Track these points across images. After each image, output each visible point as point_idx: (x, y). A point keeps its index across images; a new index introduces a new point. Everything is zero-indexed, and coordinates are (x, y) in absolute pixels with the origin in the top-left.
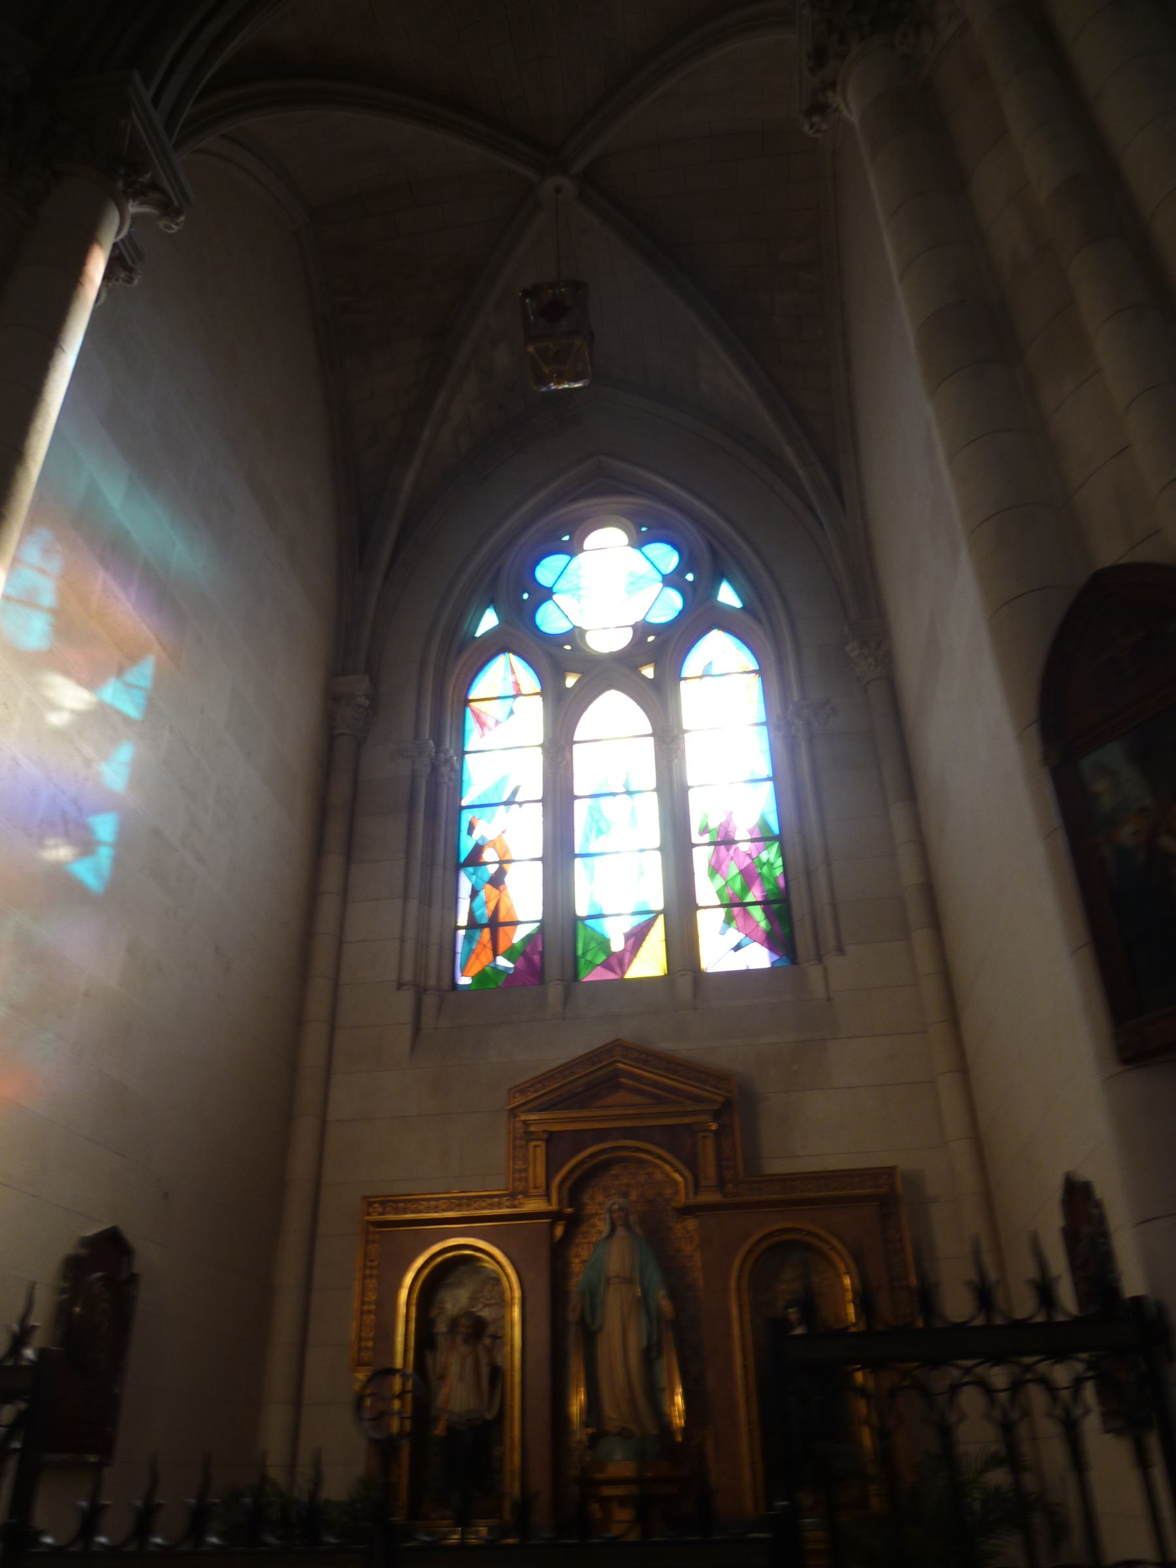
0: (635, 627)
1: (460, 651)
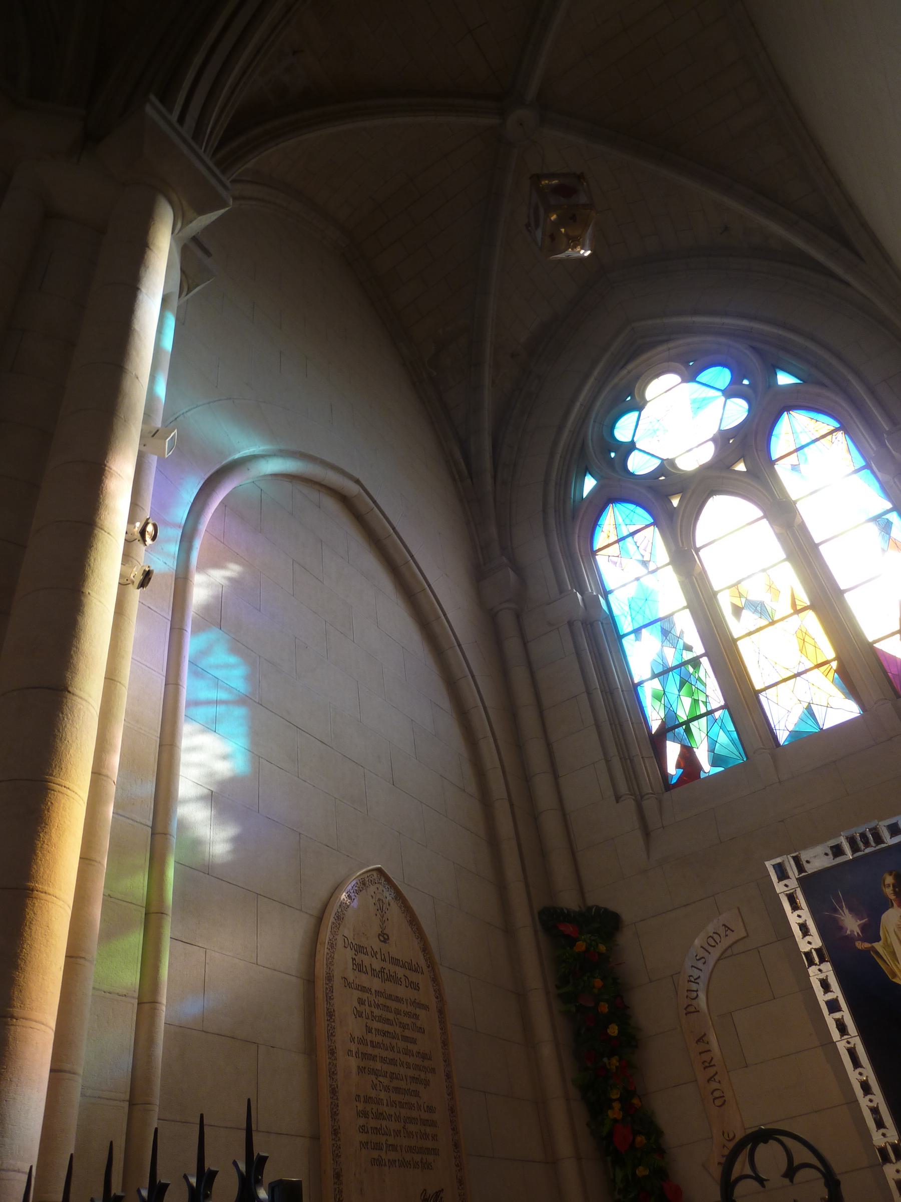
0: (714, 439)
1: (574, 517)
